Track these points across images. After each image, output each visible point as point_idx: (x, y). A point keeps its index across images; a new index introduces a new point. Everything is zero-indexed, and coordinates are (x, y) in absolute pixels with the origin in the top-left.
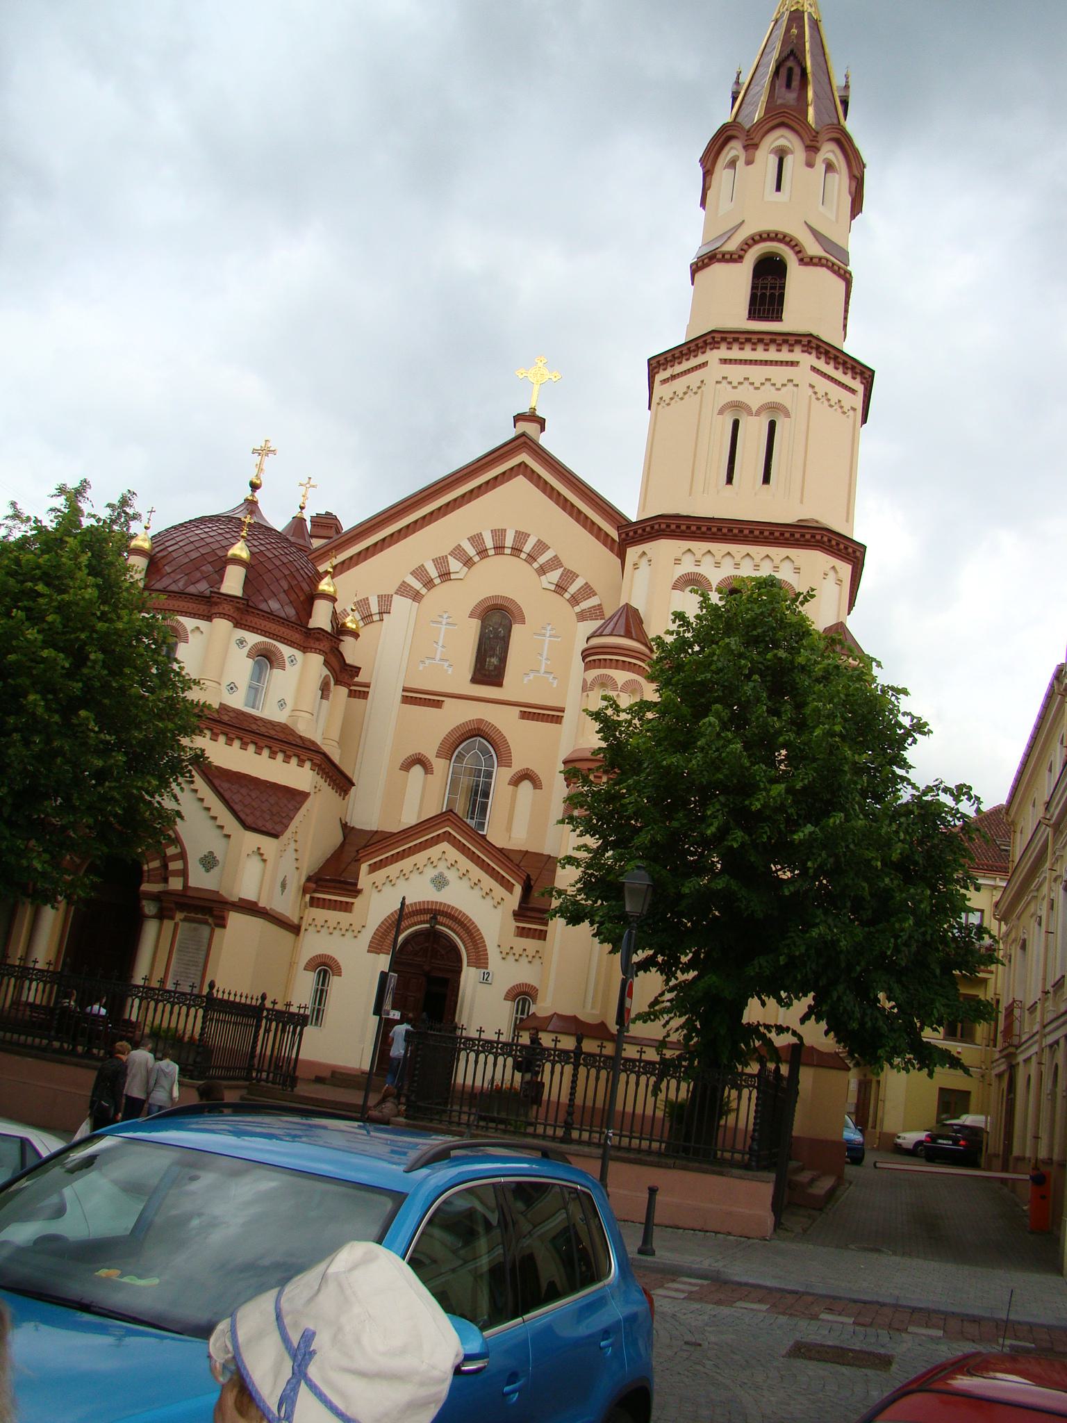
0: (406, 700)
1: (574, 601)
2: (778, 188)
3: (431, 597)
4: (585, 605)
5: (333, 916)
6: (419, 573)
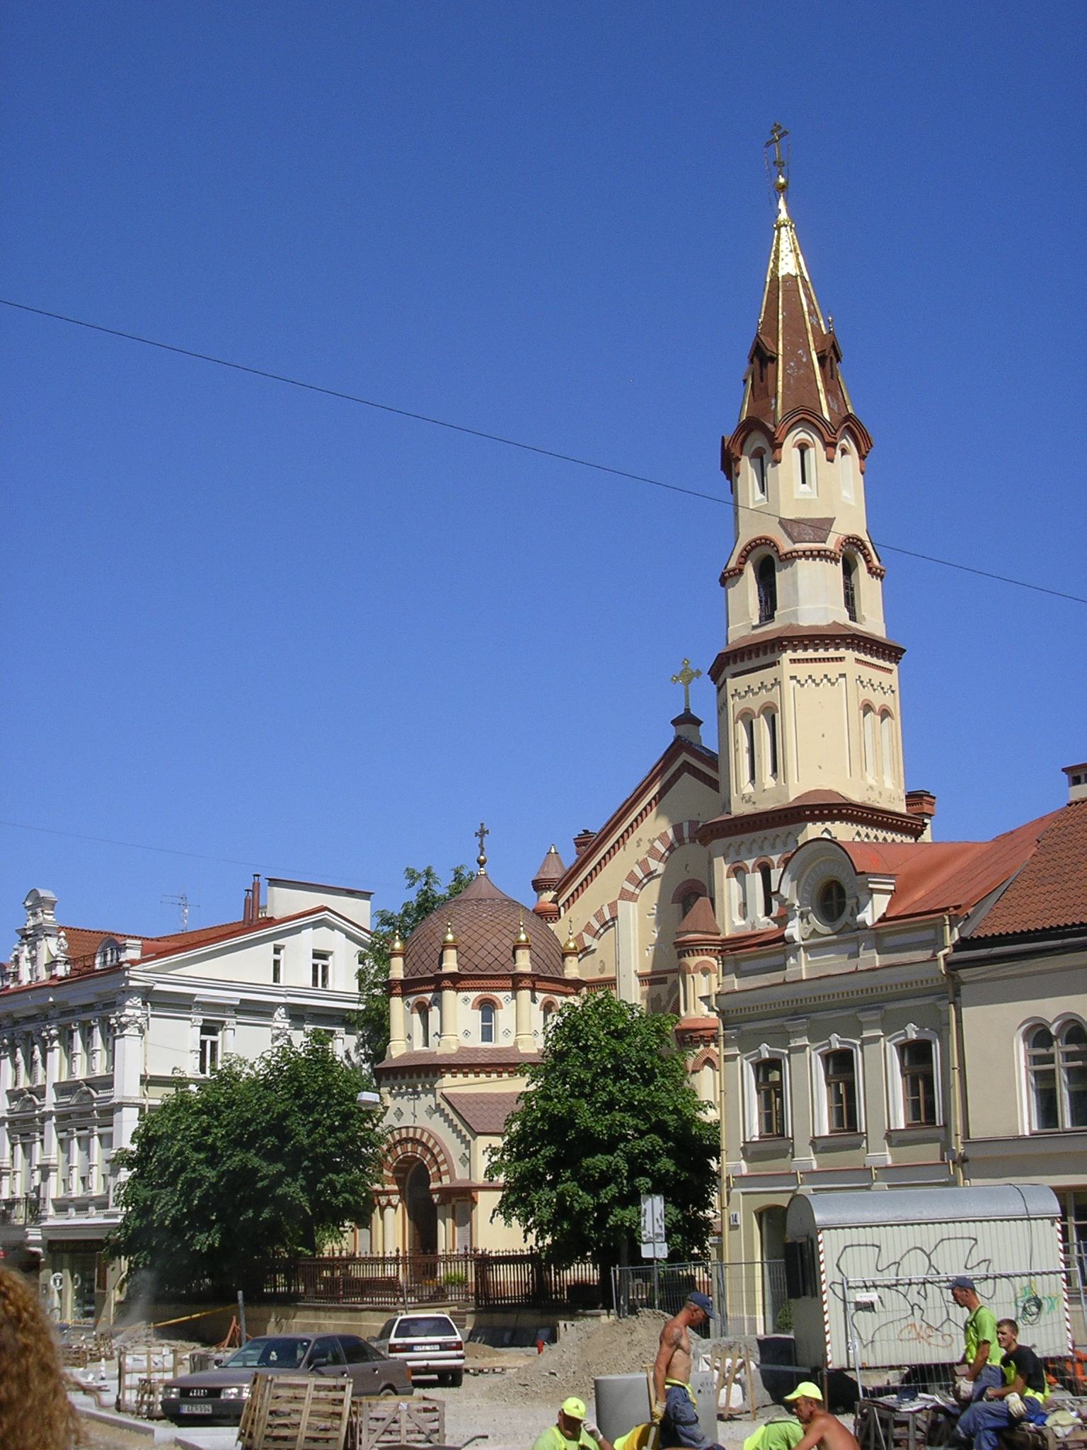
2: (804, 482)
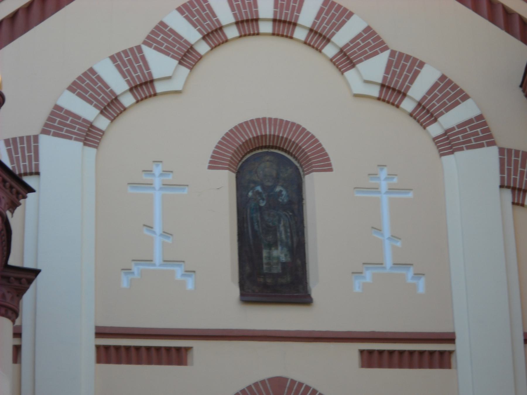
0: (106, 355)
1: (425, 114)
3: (119, 133)
4: (451, 119)
6: (87, 85)
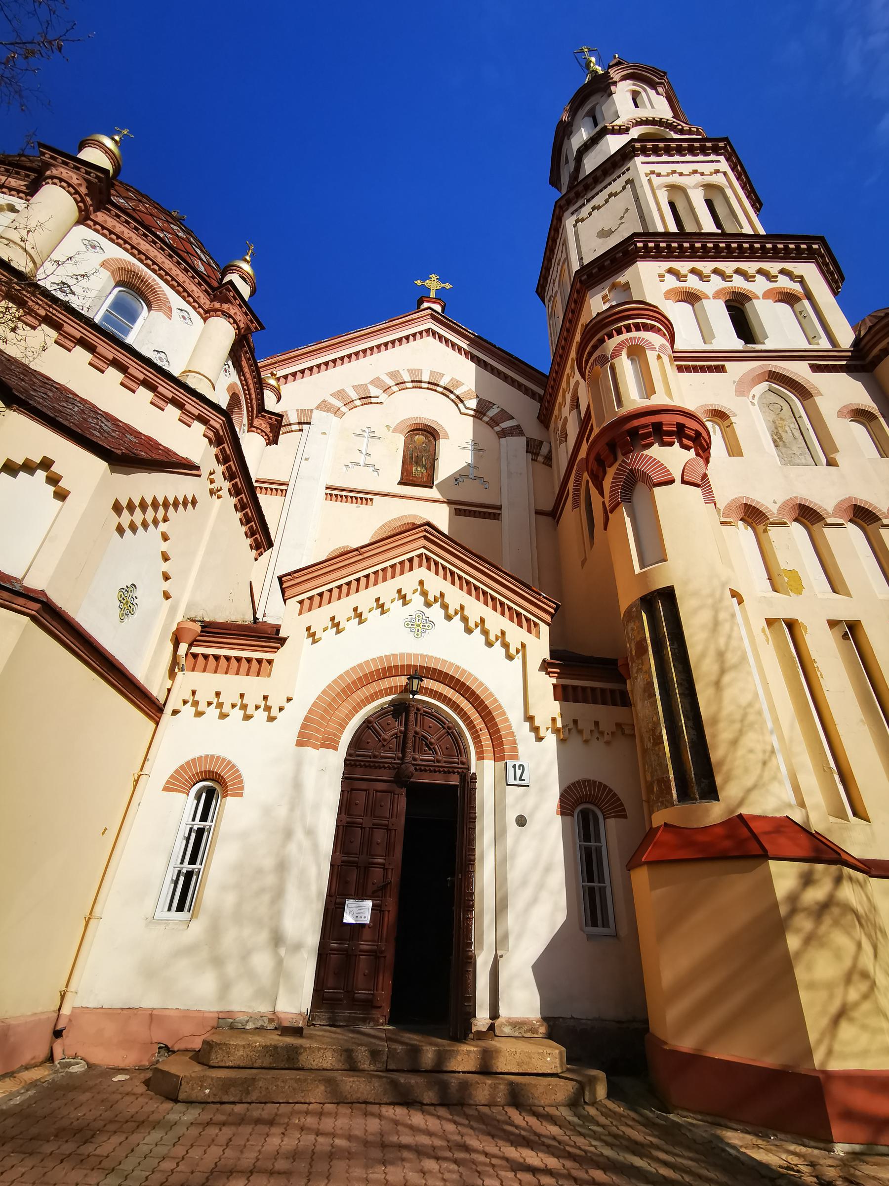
4: (505, 425)
5: (231, 685)
